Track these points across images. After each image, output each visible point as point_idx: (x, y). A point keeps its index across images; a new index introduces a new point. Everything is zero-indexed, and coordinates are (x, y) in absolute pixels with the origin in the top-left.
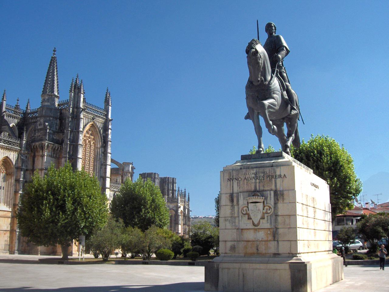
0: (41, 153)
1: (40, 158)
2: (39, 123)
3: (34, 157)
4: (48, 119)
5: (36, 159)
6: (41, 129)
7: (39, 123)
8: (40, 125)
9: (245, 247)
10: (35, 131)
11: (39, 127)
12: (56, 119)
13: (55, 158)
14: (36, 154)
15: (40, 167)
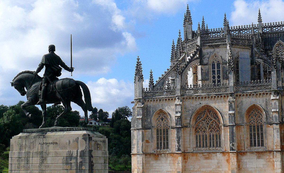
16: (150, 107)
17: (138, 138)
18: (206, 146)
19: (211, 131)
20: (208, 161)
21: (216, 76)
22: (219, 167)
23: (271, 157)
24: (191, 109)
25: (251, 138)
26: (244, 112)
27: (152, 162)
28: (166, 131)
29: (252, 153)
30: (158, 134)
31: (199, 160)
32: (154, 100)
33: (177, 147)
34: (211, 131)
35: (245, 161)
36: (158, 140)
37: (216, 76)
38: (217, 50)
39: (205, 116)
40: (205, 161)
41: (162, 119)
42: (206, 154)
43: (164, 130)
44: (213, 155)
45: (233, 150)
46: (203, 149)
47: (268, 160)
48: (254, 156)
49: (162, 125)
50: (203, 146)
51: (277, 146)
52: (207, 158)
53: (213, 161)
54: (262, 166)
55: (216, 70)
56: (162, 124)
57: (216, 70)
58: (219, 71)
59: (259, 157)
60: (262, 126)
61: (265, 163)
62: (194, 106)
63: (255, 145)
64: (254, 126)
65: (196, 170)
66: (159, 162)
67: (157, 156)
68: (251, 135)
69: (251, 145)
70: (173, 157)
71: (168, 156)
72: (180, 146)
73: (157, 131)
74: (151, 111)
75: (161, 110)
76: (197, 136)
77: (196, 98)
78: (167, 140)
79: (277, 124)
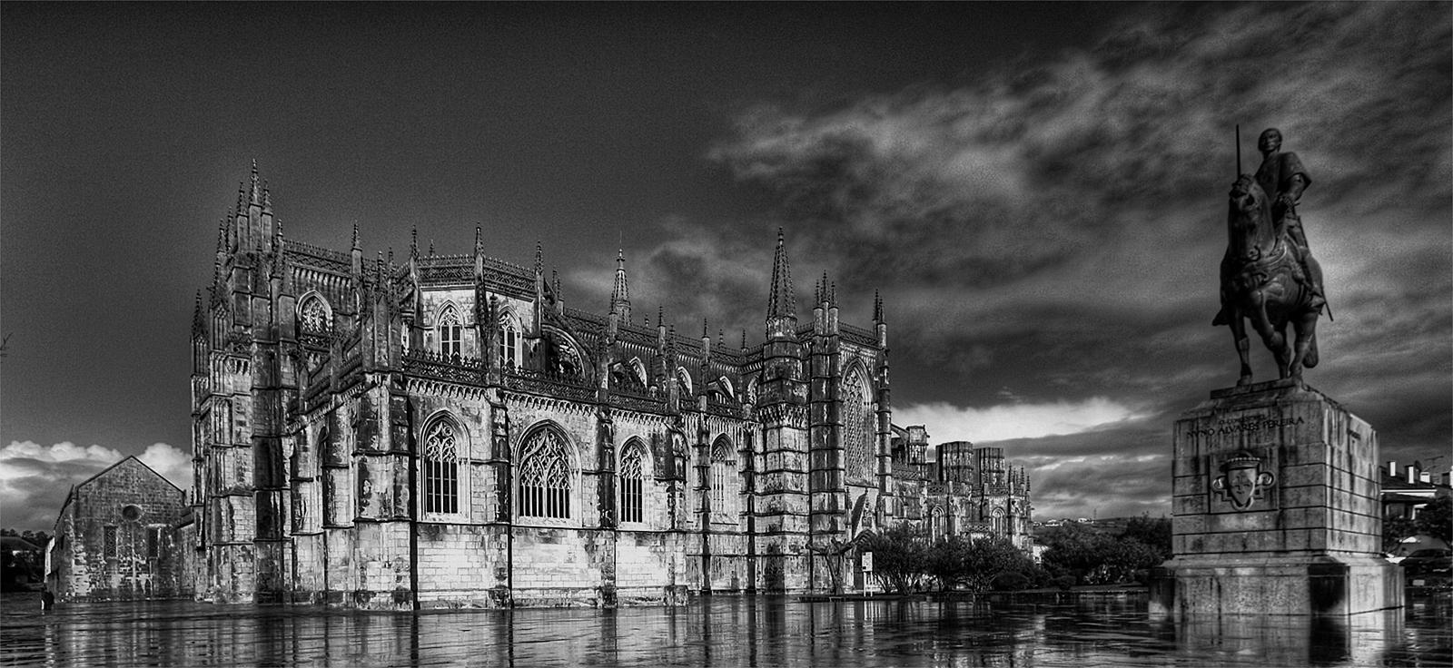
0: (776, 424)
6: (771, 381)
15: (776, 447)
17: (399, 480)
18: (541, 515)
20: (551, 546)
22: (570, 561)
23: (658, 543)
31: (532, 543)
33: (497, 509)
39: (540, 444)
40: (544, 546)
42: (546, 530)
43: (446, 464)
44: (559, 532)
46: (537, 519)
47: (653, 549)
48: (632, 541)
50: (535, 515)
52: (547, 541)
54: (643, 560)
56: (441, 450)
59: (639, 543)
61: (649, 554)
62: (524, 417)
65: (524, 566)
66: (439, 544)
67: (436, 532)
69: (623, 520)
70: (474, 533)
71: (463, 532)
76: (521, 488)
78: (454, 492)
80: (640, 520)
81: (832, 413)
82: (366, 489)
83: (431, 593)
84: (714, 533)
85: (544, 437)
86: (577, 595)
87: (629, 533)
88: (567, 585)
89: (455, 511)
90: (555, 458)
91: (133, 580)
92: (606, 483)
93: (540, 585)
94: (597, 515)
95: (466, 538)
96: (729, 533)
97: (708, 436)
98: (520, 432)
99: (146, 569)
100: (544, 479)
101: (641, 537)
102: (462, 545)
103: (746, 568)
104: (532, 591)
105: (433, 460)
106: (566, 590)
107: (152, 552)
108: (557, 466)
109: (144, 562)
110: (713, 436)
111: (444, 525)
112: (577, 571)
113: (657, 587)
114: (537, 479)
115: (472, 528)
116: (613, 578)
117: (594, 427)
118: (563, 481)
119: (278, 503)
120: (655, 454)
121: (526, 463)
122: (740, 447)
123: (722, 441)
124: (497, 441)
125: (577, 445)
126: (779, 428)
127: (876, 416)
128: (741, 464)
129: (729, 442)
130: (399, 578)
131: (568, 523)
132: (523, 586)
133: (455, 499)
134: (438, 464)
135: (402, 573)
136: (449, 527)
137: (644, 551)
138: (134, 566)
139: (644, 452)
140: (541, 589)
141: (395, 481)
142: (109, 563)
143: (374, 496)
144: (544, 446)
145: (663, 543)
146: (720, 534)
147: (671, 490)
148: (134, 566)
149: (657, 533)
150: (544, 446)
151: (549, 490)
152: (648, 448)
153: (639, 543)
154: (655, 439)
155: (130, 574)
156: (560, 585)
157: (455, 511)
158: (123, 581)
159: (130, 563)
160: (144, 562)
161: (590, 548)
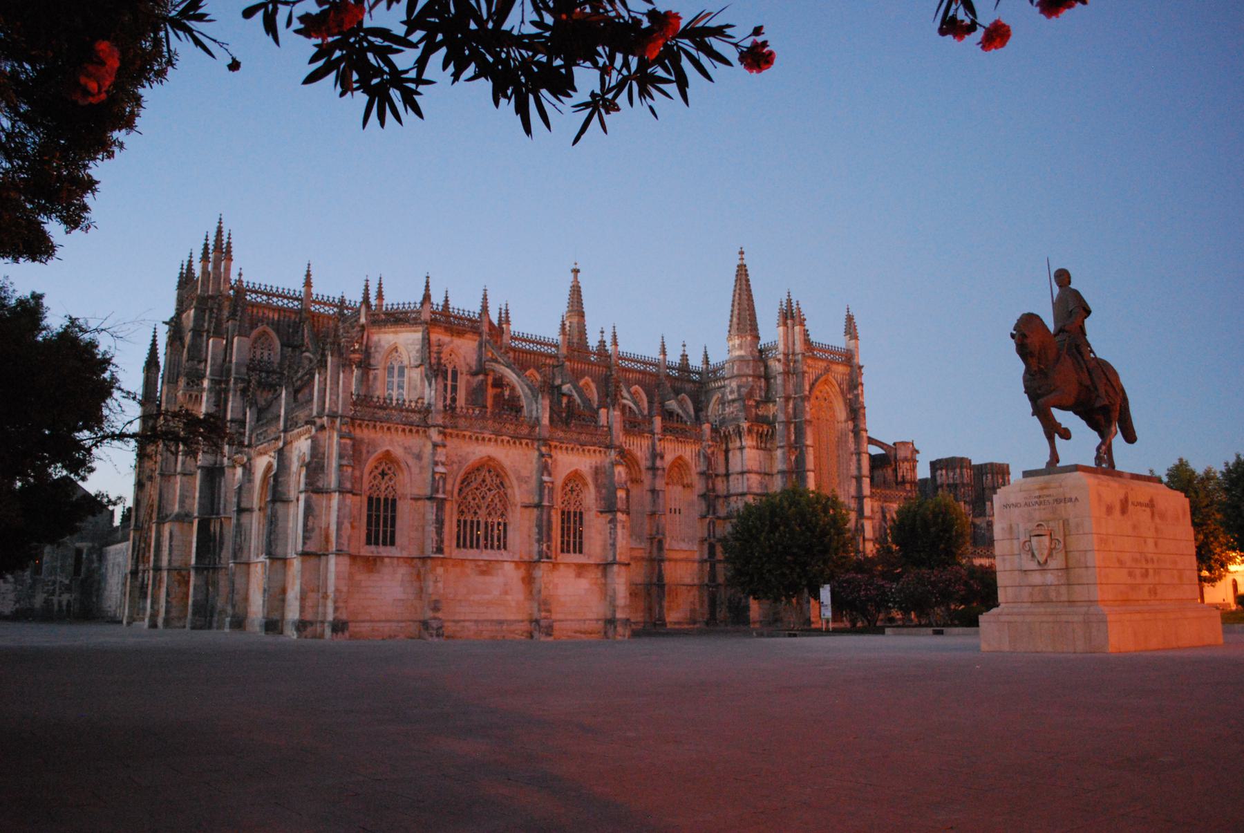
0: (738, 444)
1: (738, 453)
2: (728, 390)
3: (727, 451)
4: (744, 379)
5: (730, 454)
6: (733, 401)
7: (728, 390)
8: (732, 392)
9: (1031, 594)
10: (723, 404)
11: (730, 397)
12: (759, 377)
13: (765, 449)
14: (731, 446)
15: (738, 469)
16: (362, 440)
18: (478, 547)
19: (490, 514)
20: (487, 578)
21: (449, 396)
22: (506, 593)
23: (599, 575)
24: (456, 459)
25: (562, 536)
26: (559, 482)
27: (358, 577)
28: (392, 504)
29: (568, 565)
30: (370, 509)
32: (375, 427)
34: (490, 514)
35: (556, 581)
36: (369, 523)
37: (449, 396)
38: (458, 342)
39: (479, 480)
40: (480, 579)
41: (383, 474)
43: (386, 500)
45: (548, 557)
48: (571, 573)
49: (383, 487)
50: (471, 547)
51: (621, 554)
52: (483, 573)
53: (495, 579)
55: (449, 382)
57: (449, 382)
58: (454, 389)
59: (579, 575)
60: (581, 513)
61: (587, 586)
63: (568, 552)
64: (569, 512)
67: (372, 564)
68: (563, 529)
69: (562, 551)
72: (442, 541)
73: (370, 499)
74: (364, 452)
75: (388, 451)
76: (459, 521)
77: (470, 437)
78: (393, 525)
79: (623, 512)
80: (581, 552)
81: (800, 433)
82: (310, 524)
83: (367, 624)
84: (670, 560)
85: (484, 473)
86: (513, 627)
87: (568, 565)
88: (502, 617)
89: (393, 543)
90: (494, 492)
91: (55, 599)
92: (545, 517)
93: (474, 617)
94: (535, 548)
95: (403, 571)
96: (686, 560)
97: (662, 458)
98: (460, 468)
99: (68, 589)
100: (483, 512)
101: (581, 569)
102: (399, 576)
103: (706, 599)
104: (467, 624)
105: (375, 496)
106: (501, 622)
107: (77, 571)
108: (497, 501)
109: (67, 582)
110: (669, 458)
111: (382, 558)
112: (513, 604)
113: (597, 620)
114: (475, 513)
115: (409, 560)
116: (549, 611)
117: (534, 461)
118: (502, 515)
119: (218, 529)
120: (597, 486)
121: (465, 498)
122: (699, 470)
123: (679, 463)
124: (437, 477)
125: (517, 479)
126: (741, 448)
127: (851, 435)
128: (699, 486)
129: (686, 464)
130: (336, 609)
131: (504, 555)
132: (457, 618)
133: (393, 533)
134: (378, 500)
135: (341, 604)
136: (387, 560)
137: (584, 584)
138: (57, 586)
139: (585, 484)
140: (476, 621)
141: (338, 517)
142: (35, 582)
143: (317, 530)
144: (484, 481)
145: (605, 575)
146: (676, 561)
147: (613, 521)
148: (57, 586)
149: (598, 565)
150: (484, 481)
151: (486, 523)
152: (589, 480)
153: (579, 575)
154: (597, 471)
155: (53, 594)
156: (495, 617)
157: (393, 543)
158: (46, 601)
159: (54, 583)
160: (67, 582)
161: (529, 580)
